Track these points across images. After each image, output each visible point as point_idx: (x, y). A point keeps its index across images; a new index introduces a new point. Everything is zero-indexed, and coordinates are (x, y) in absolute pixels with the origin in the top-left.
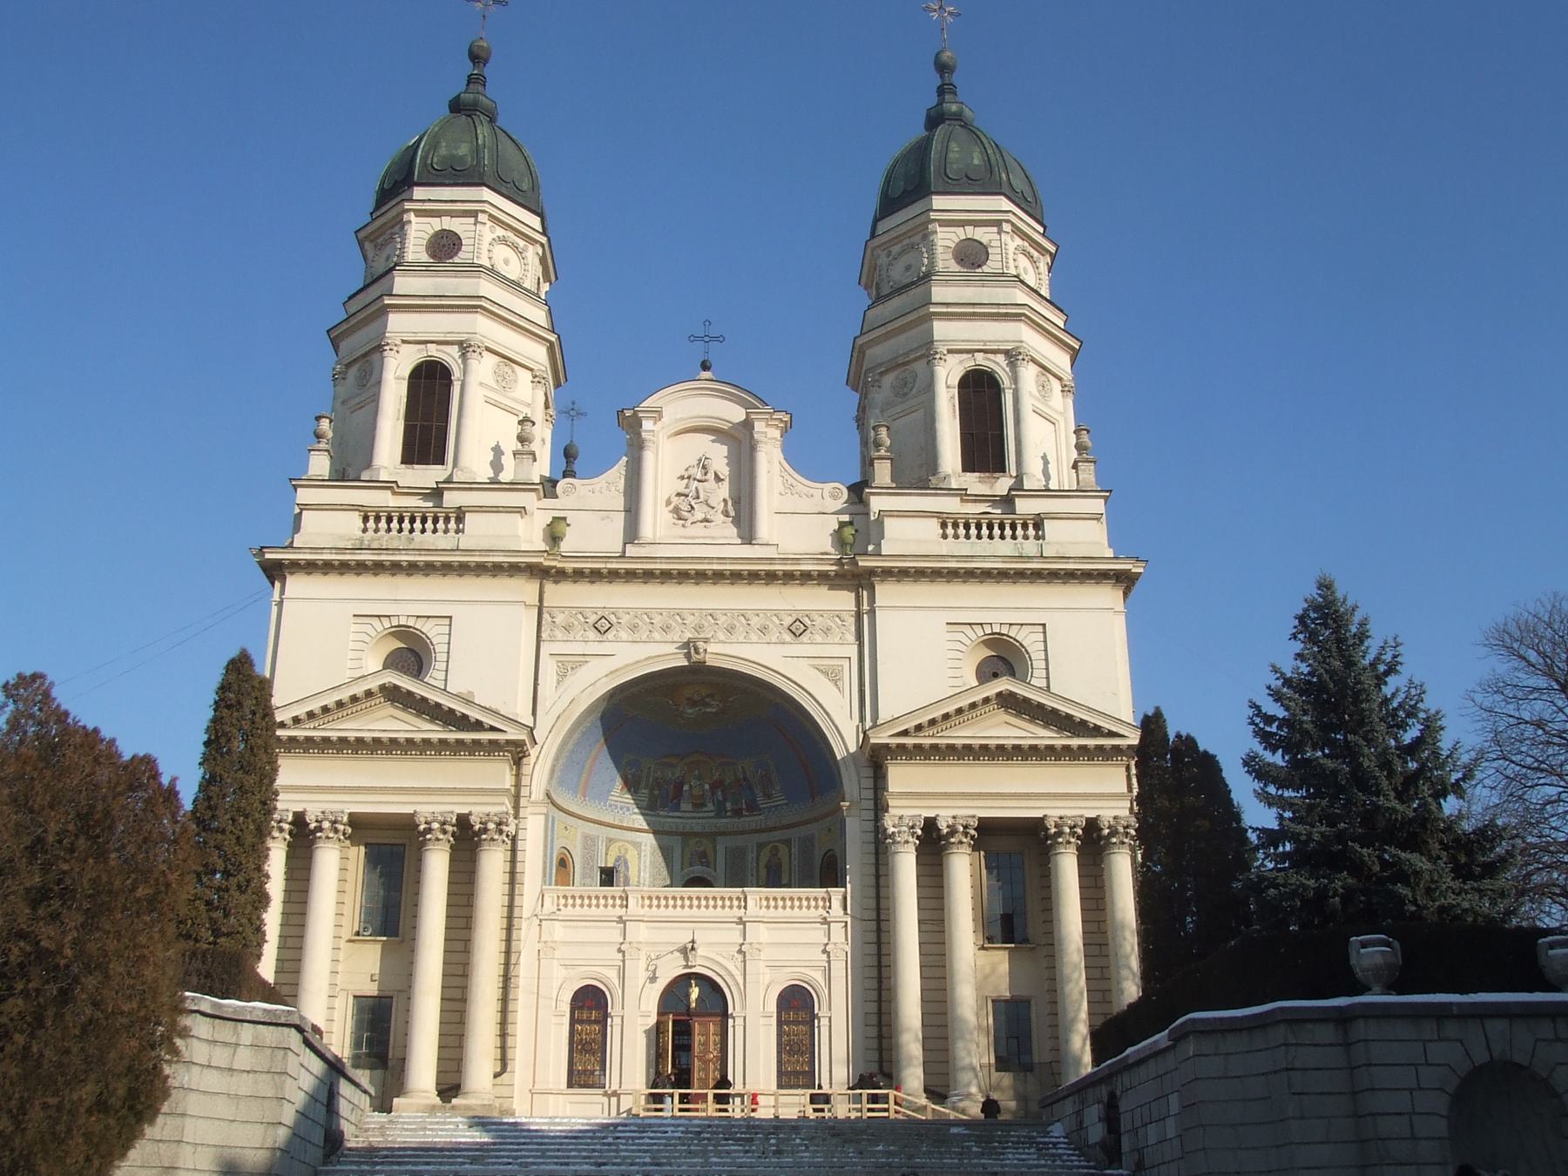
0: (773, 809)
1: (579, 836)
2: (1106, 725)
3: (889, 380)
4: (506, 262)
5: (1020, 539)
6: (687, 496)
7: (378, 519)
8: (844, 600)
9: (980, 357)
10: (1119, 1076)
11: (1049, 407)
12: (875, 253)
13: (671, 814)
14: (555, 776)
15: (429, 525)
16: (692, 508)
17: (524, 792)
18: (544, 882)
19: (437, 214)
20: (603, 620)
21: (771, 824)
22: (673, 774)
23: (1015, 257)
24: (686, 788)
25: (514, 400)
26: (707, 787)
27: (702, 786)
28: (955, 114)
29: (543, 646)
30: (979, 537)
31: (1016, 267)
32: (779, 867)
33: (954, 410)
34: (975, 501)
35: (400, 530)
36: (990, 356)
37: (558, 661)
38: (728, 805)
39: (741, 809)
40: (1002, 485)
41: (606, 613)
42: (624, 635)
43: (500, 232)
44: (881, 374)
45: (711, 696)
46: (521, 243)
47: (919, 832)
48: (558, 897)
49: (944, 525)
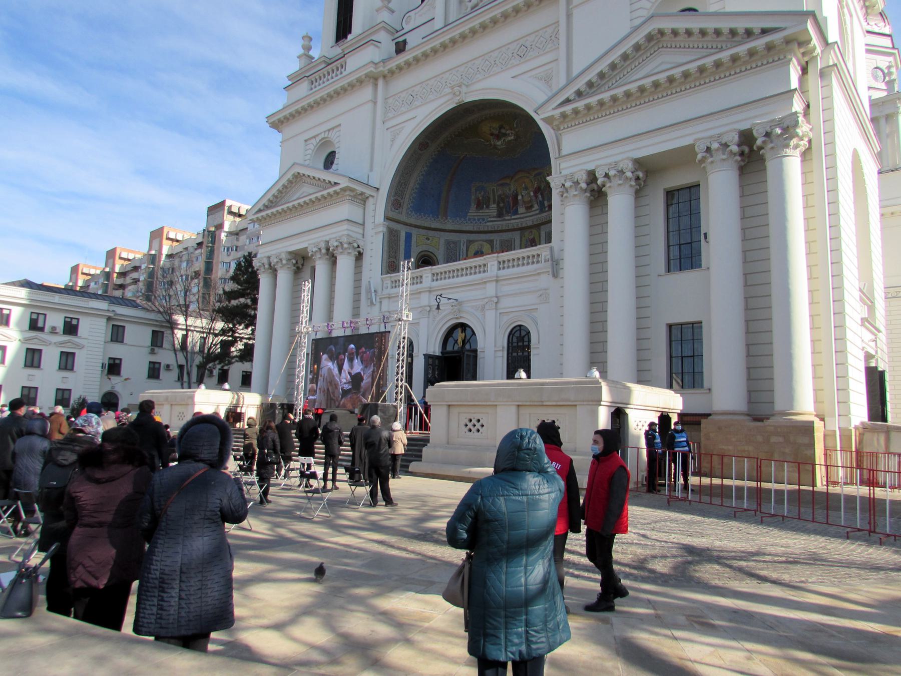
1: (442, 242)
13: (513, 217)
24: (520, 197)
26: (532, 194)
27: (529, 193)
45: (501, 127)
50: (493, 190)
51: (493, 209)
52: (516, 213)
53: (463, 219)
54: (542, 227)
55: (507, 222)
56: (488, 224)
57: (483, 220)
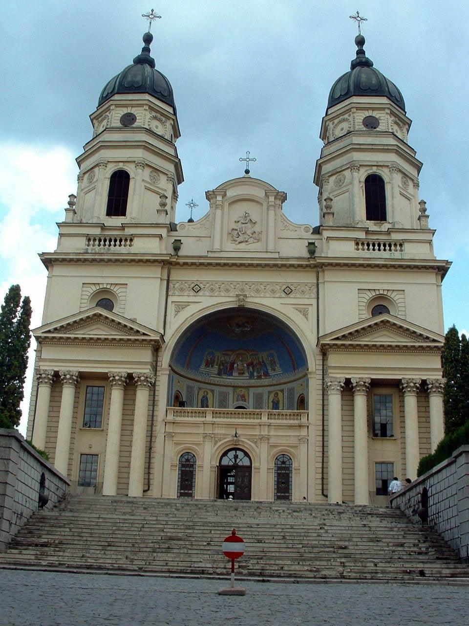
0: (276, 376)
2: (432, 337)
3: (332, 179)
4: (157, 127)
5: (393, 251)
6: (237, 230)
7: (95, 240)
8: (309, 278)
9: (374, 169)
10: (428, 480)
11: (408, 192)
12: (327, 123)
13: (228, 377)
14: (174, 358)
15: (118, 243)
16: (239, 235)
17: (159, 364)
18: (168, 405)
19: (126, 106)
20: (197, 286)
21: (275, 383)
22: (230, 359)
23: (392, 127)
24: (235, 365)
25: (160, 188)
26: (245, 365)
28: (365, 62)
29: (170, 299)
30: (374, 250)
31: (392, 129)
32: (278, 402)
33: (363, 193)
34: (372, 234)
35: (105, 245)
36: (380, 168)
37: (175, 305)
38: (255, 374)
39: (261, 376)
40: (385, 227)
41: (198, 284)
42: (207, 294)
43: (154, 114)
44: (329, 176)
46: (164, 119)
47: (343, 385)
48: (174, 412)
49: (357, 244)
50: (219, 356)
51: (215, 369)
52: (231, 375)
53: (196, 372)
54: (251, 389)
55: (224, 380)
56: (211, 378)
57: (208, 375)
